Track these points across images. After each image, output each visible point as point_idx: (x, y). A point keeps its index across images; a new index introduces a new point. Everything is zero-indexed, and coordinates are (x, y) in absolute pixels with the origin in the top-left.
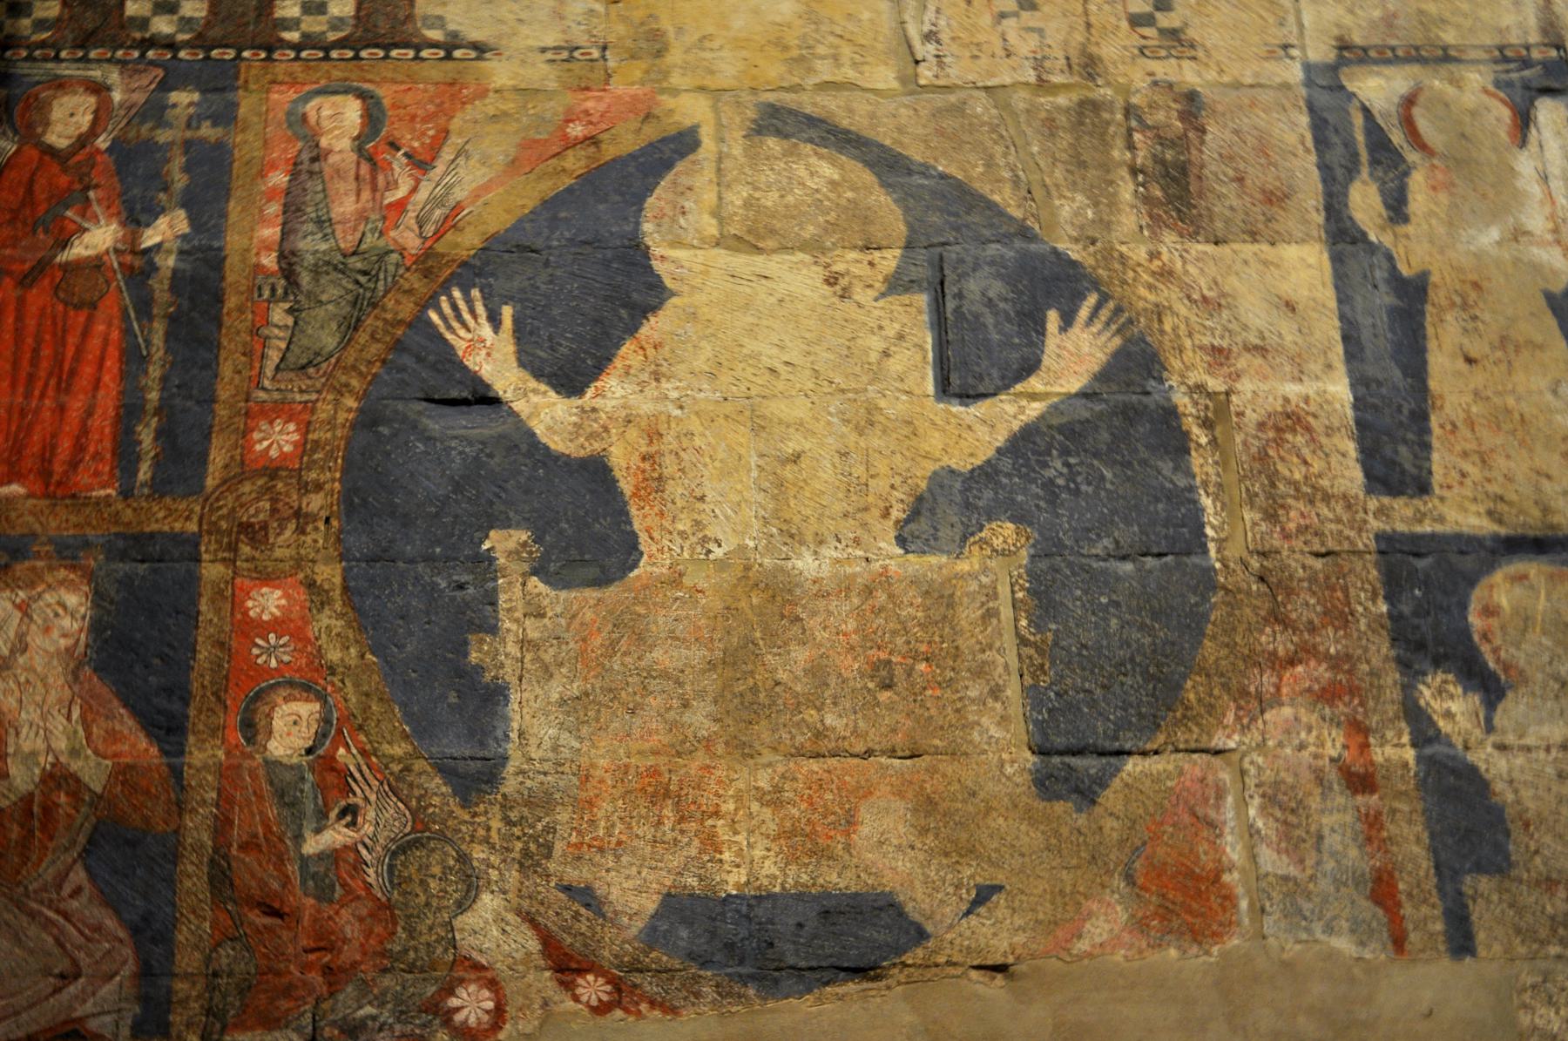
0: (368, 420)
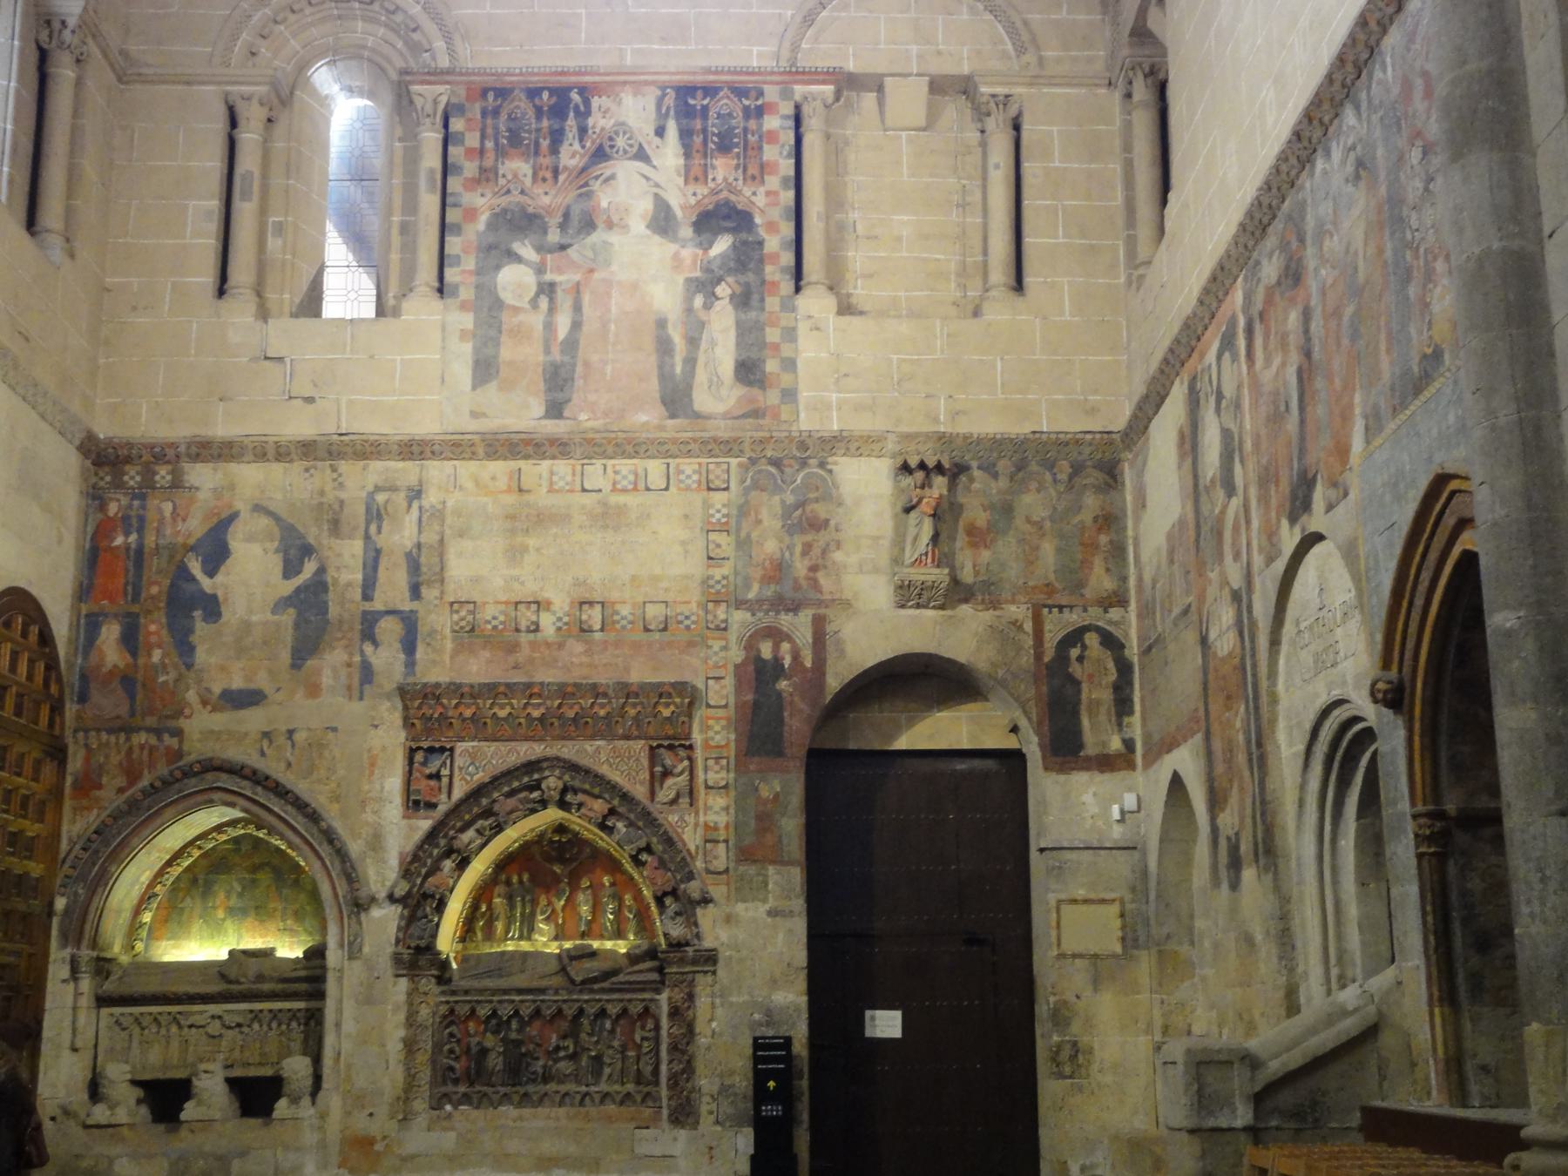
0: (172, 585)
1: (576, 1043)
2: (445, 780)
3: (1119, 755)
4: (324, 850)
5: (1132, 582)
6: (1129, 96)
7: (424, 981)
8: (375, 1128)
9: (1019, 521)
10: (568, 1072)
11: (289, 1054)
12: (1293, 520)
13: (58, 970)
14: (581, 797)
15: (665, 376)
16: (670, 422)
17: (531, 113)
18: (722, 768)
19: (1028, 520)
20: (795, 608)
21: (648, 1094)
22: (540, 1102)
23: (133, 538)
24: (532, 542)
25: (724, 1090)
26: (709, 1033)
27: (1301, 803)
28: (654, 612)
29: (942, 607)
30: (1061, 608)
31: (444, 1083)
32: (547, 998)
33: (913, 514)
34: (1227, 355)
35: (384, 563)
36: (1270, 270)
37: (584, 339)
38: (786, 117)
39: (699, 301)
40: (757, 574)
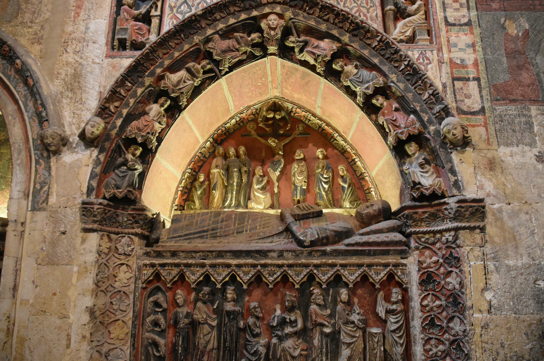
1: (306, 316)
2: (155, 22)
4: (20, 92)
7: (125, 240)
10: (296, 353)
18: (461, 5)
26: (485, 307)
32: (269, 261)
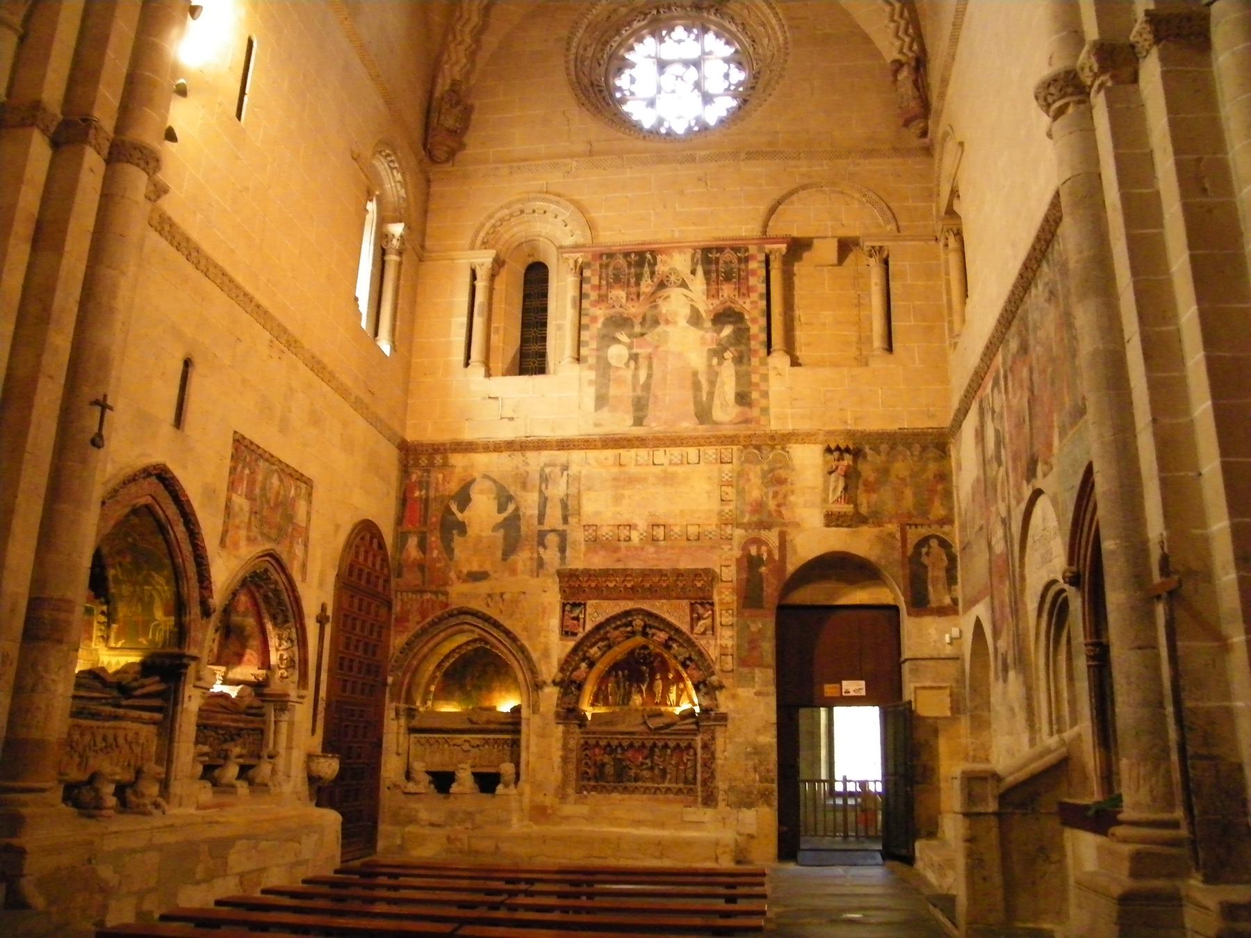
2: (582, 621)
3: (949, 606)
4: (519, 656)
5: (956, 510)
6: (946, 245)
8: (548, 800)
9: (893, 478)
11: (504, 761)
12: (1028, 481)
13: (390, 714)
14: (654, 631)
15: (697, 401)
16: (700, 427)
17: (625, 265)
19: (897, 477)
20: (768, 527)
21: (691, 789)
22: (633, 792)
23: (423, 492)
24: (626, 493)
25: (731, 789)
27: (1037, 634)
28: (693, 530)
29: (849, 526)
30: (916, 526)
31: (583, 779)
33: (833, 475)
34: (996, 390)
35: (549, 505)
36: (1014, 345)
37: (653, 382)
38: (760, 262)
39: (715, 361)
40: (748, 508)
